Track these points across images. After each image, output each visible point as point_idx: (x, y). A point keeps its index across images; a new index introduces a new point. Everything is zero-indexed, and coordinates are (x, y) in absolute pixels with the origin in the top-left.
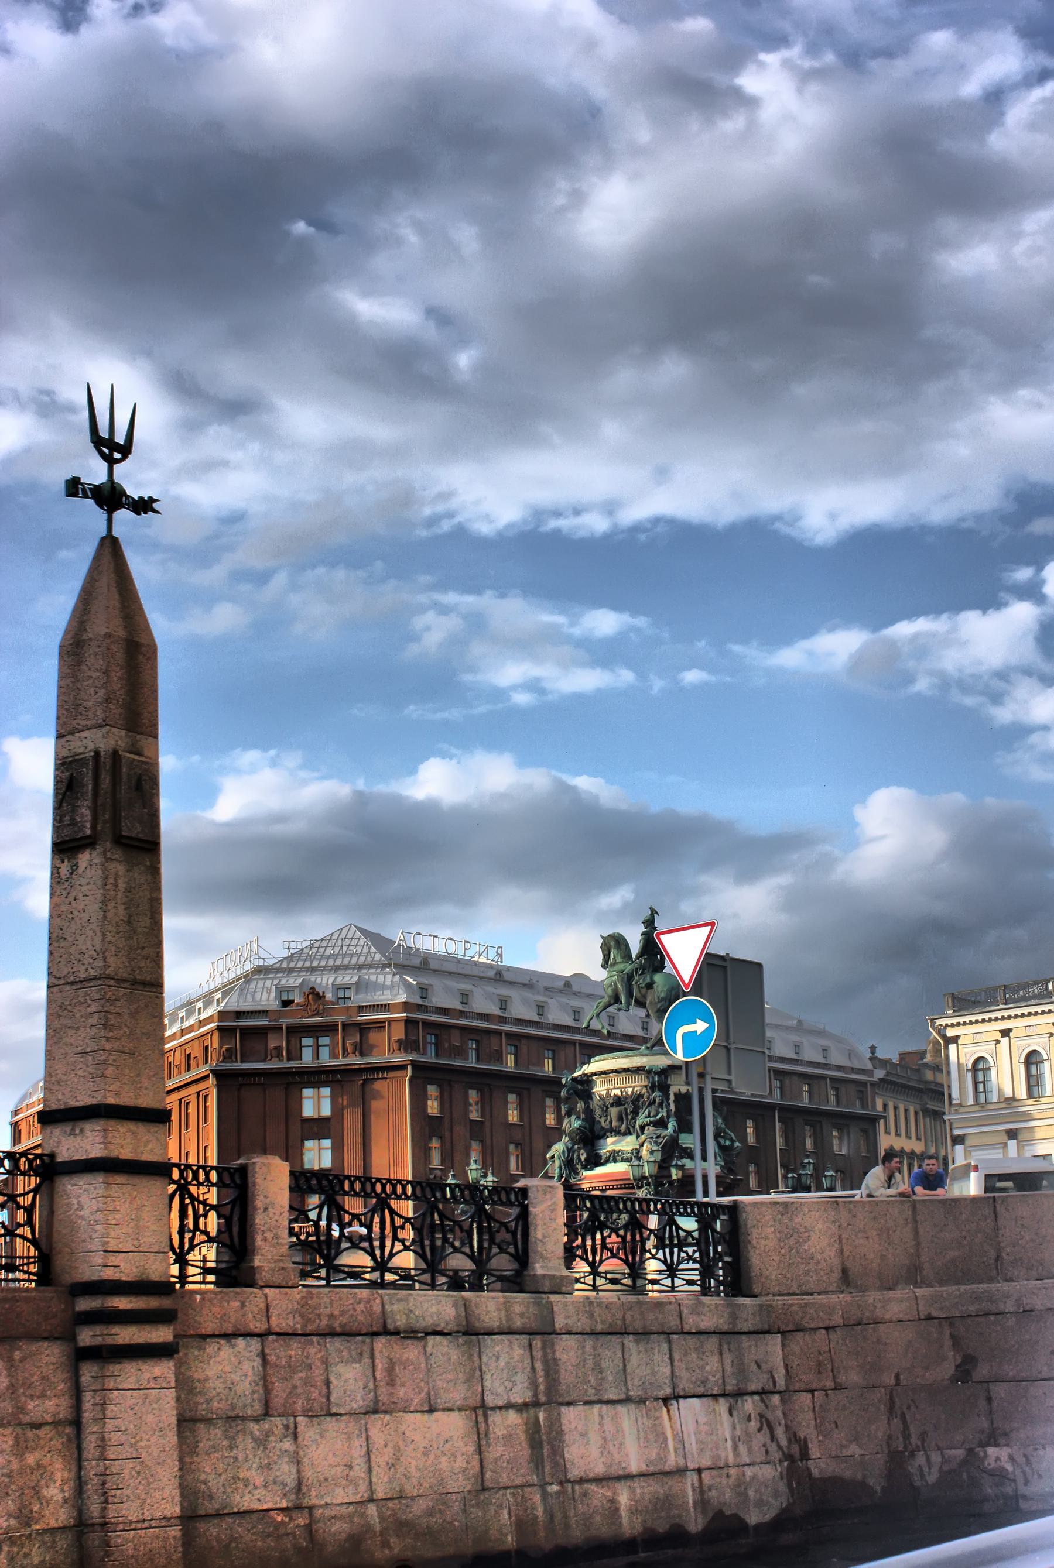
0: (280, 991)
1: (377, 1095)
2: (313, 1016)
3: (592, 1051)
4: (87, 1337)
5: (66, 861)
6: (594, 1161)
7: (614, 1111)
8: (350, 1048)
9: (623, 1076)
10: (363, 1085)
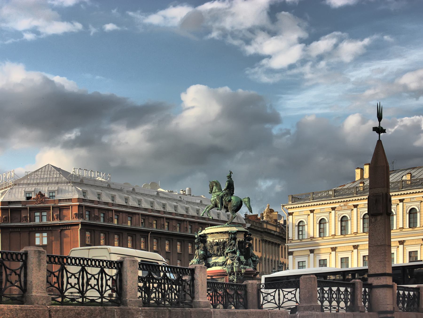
0: (26, 193)
1: (66, 236)
2: (40, 203)
3: (204, 226)
5: (373, 218)
6: (208, 266)
7: (215, 248)
8: (55, 217)
9: (220, 234)
10: (60, 232)
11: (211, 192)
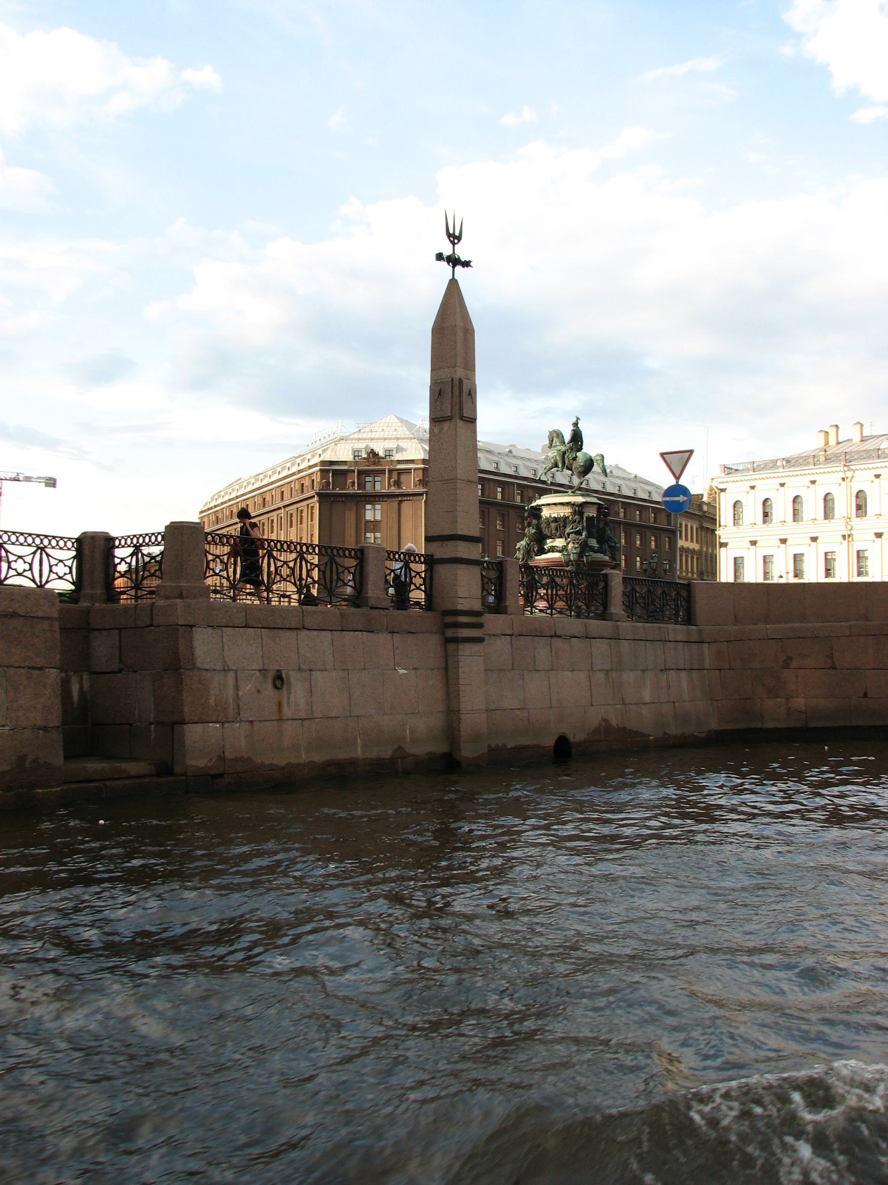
4: (450, 633)
6: (542, 551)
7: (553, 525)
8: (392, 483)
11: (551, 446)
